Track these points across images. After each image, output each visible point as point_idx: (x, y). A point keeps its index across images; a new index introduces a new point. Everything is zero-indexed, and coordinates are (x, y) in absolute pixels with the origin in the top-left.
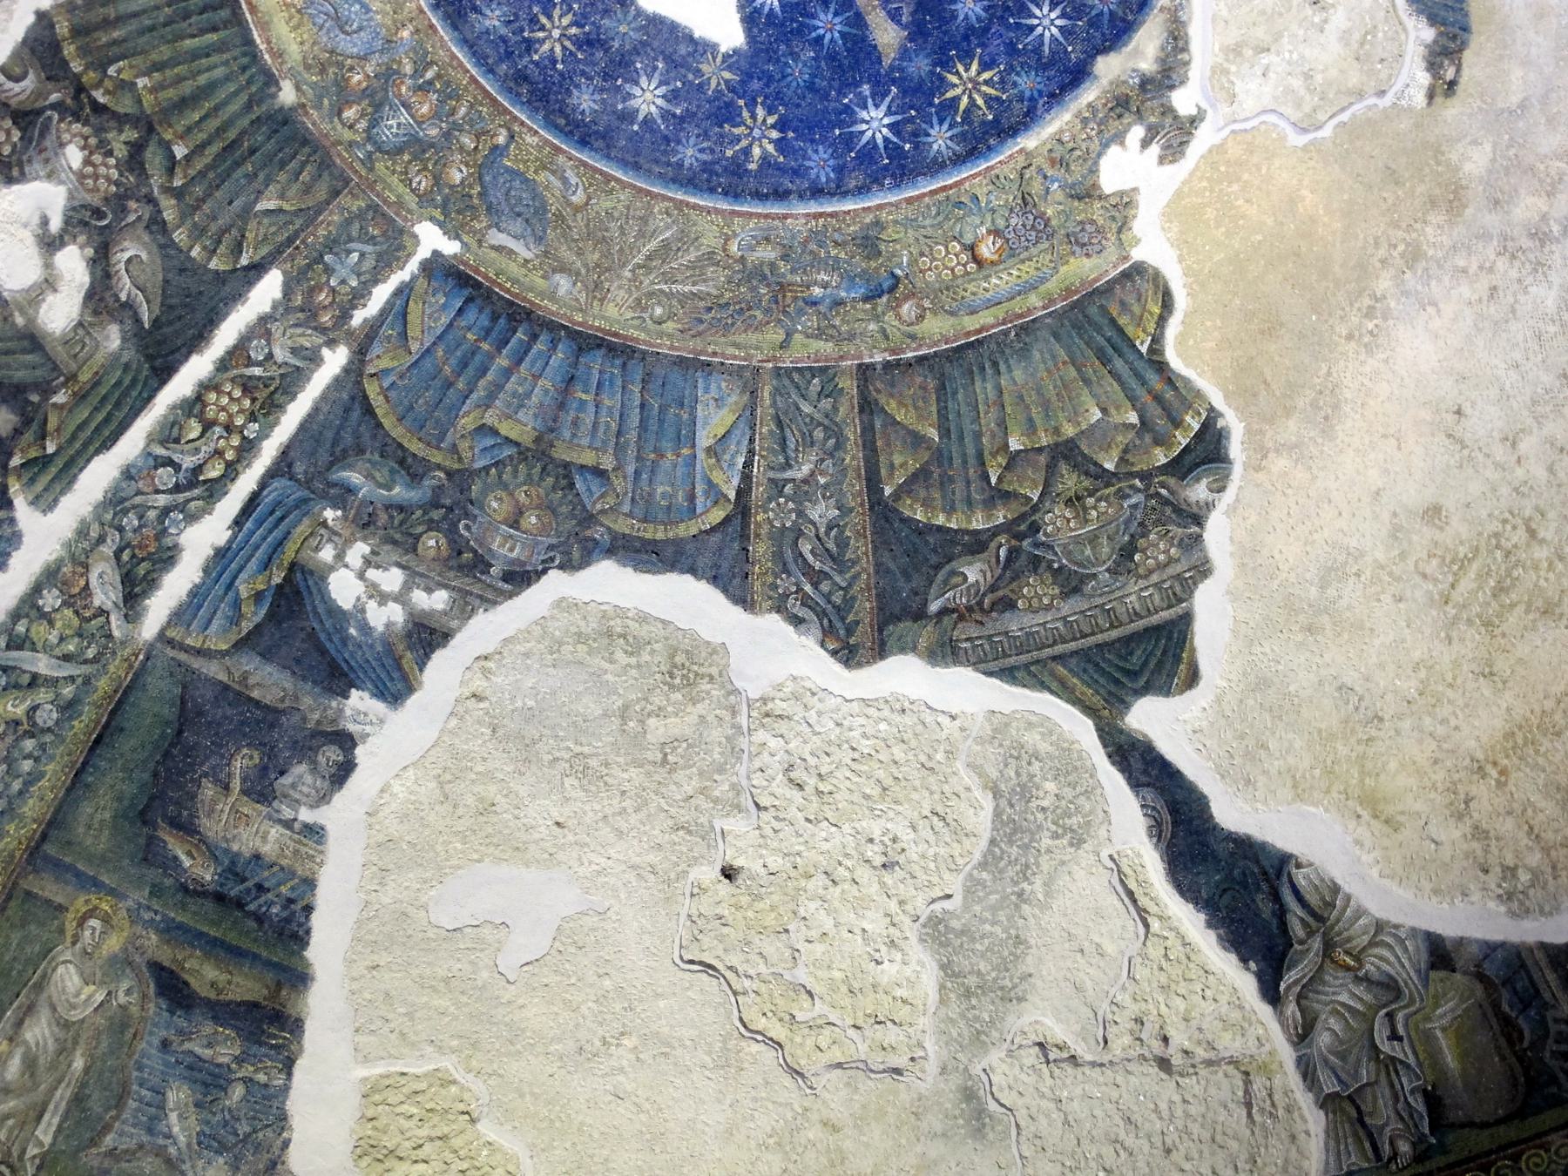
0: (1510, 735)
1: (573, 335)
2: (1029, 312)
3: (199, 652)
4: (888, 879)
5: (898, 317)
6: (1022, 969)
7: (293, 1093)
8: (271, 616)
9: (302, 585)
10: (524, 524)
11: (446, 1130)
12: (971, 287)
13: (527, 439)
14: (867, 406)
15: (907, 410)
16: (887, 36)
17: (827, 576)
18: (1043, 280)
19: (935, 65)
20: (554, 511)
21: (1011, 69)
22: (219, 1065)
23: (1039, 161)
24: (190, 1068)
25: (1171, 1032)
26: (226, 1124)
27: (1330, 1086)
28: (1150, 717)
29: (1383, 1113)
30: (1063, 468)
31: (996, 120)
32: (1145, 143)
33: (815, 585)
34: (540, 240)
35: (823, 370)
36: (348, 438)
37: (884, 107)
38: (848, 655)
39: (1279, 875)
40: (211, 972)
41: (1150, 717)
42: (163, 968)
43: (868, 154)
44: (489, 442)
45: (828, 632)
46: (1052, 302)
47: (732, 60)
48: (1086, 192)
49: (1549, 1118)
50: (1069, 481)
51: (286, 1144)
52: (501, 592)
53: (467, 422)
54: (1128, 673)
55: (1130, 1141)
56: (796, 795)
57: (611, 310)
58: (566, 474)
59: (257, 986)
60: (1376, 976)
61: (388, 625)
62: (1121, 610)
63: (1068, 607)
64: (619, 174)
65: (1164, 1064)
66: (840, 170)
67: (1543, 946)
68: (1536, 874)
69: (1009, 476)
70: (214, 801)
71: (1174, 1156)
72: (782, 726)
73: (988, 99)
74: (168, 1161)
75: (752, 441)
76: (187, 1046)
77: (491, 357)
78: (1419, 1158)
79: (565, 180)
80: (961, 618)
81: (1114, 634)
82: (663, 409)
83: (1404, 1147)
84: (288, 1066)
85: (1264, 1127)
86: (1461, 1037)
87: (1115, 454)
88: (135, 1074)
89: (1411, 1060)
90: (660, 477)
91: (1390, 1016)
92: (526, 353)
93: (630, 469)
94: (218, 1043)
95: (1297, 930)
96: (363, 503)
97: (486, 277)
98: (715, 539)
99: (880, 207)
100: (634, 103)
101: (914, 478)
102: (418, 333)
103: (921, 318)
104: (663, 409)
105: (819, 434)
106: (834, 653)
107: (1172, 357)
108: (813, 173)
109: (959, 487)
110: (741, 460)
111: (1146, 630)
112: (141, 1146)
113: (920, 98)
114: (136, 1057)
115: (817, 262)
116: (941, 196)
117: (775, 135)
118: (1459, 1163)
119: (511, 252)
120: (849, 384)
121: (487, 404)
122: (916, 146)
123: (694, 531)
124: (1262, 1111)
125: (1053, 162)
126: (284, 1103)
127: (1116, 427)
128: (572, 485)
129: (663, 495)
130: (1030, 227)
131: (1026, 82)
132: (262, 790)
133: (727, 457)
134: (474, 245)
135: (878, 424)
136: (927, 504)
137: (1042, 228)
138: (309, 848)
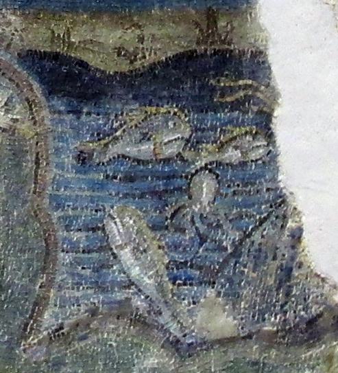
7: (282, 160)
22: (167, 161)
24: (129, 179)
26: (203, 240)
40: (111, 35)
42: (43, 56)
51: (297, 236)
59: (181, 29)
74: (141, 322)
76: (115, 150)
84: (264, 126)
88: (56, 214)
94: (156, 130)
112: (94, 312)
114: (49, 190)
126: (274, 180)
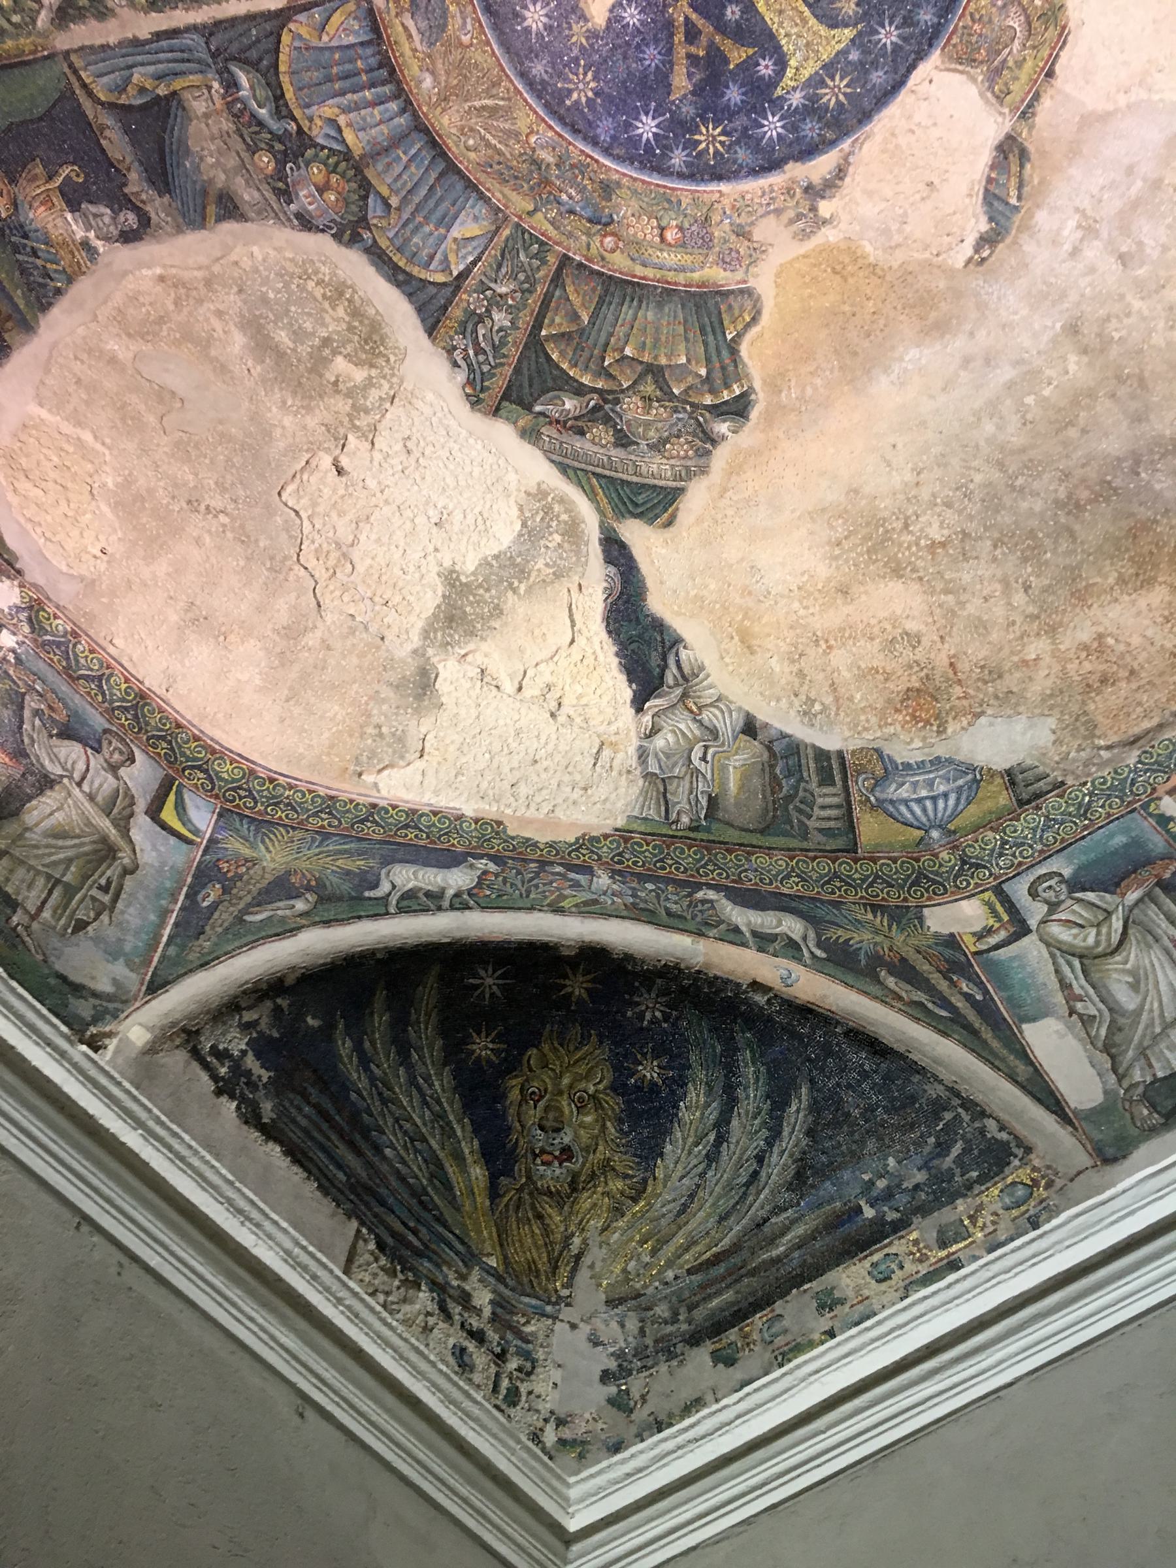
0: (842, 630)
1: (415, 116)
2: (676, 284)
3: (84, 86)
4: (435, 530)
5: (602, 242)
6: (493, 624)
8: (143, 108)
9: (173, 109)
10: (325, 196)
11: (69, 485)
12: (650, 251)
13: (357, 152)
14: (557, 279)
15: (579, 298)
16: (681, 82)
17: (485, 353)
18: (692, 271)
19: (698, 115)
20: (347, 204)
21: (738, 142)
23: (726, 202)
25: (565, 701)
27: (653, 768)
28: (634, 532)
29: (680, 796)
30: (649, 378)
31: (714, 167)
32: (791, 222)
33: (476, 355)
34: (431, 44)
35: (542, 244)
36: (254, 54)
37: (657, 121)
38: (475, 402)
39: (671, 648)
41: (634, 532)
43: (634, 141)
44: (333, 133)
45: (470, 382)
46: (690, 286)
47: (593, 35)
48: (742, 233)
49: (781, 841)
50: (649, 388)
52: (289, 220)
53: (328, 111)
54: (632, 501)
55: (514, 745)
56: (403, 457)
57: (445, 120)
58: (366, 187)
60: (706, 722)
61: (211, 181)
62: (644, 469)
63: (617, 453)
64: (495, 47)
65: (553, 715)
66: (614, 138)
67: (814, 746)
68: (825, 708)
69: (616, 366)
70: (35, 178)
71: (538, 766)
72: (414, 413)
73: (716, 152)
75: (483, 253)
77: (362, 88)
78: (691, 829)
79: (465, 23)
80: (550, 423)
81: (635, 479)
82: (441, 199)
83: (685, 819)
85: (600, 775)
86: (745, 778)
87: (683, 387)
89: (709, 776)
90: (419, 235)
91: (706, 747)
92: (382, 103)
93: (405, 216)
95: (669, 679)
96: (238, 100)
97: (388, 37)
98: (432, 290)
99: (625, 175)
100: (527, 14)
101: (563, 335)
102: (332, 33)
103: (613, 251)
104: (441, 199)
105: (521, 276)
106: (468, 395)
107: (744, 350)
108: (599, 131)
109: (586, 354)
110: (471, 259)
111: (655, 486)
113: (679, 129)
115: (573, 183)
116: (662, 190)
117: (590, 94)
118: (714, 842)
119: (410, 36)
120: (552, 260)
121: (346, 110)
122: (663, 154)
123: (422, 276)
124: (603, 767)
125: (733, 206)
127: (691, 372)
128: (366, 197)
129: (416, 245)
130: (699, 237)
131: (742, 155)
132: (73, 198)
133: (464, 251)
134: (393, 13)
135: (557, 293)
136: (562, 354)
137: (707, 243)
138: (81, 256)
